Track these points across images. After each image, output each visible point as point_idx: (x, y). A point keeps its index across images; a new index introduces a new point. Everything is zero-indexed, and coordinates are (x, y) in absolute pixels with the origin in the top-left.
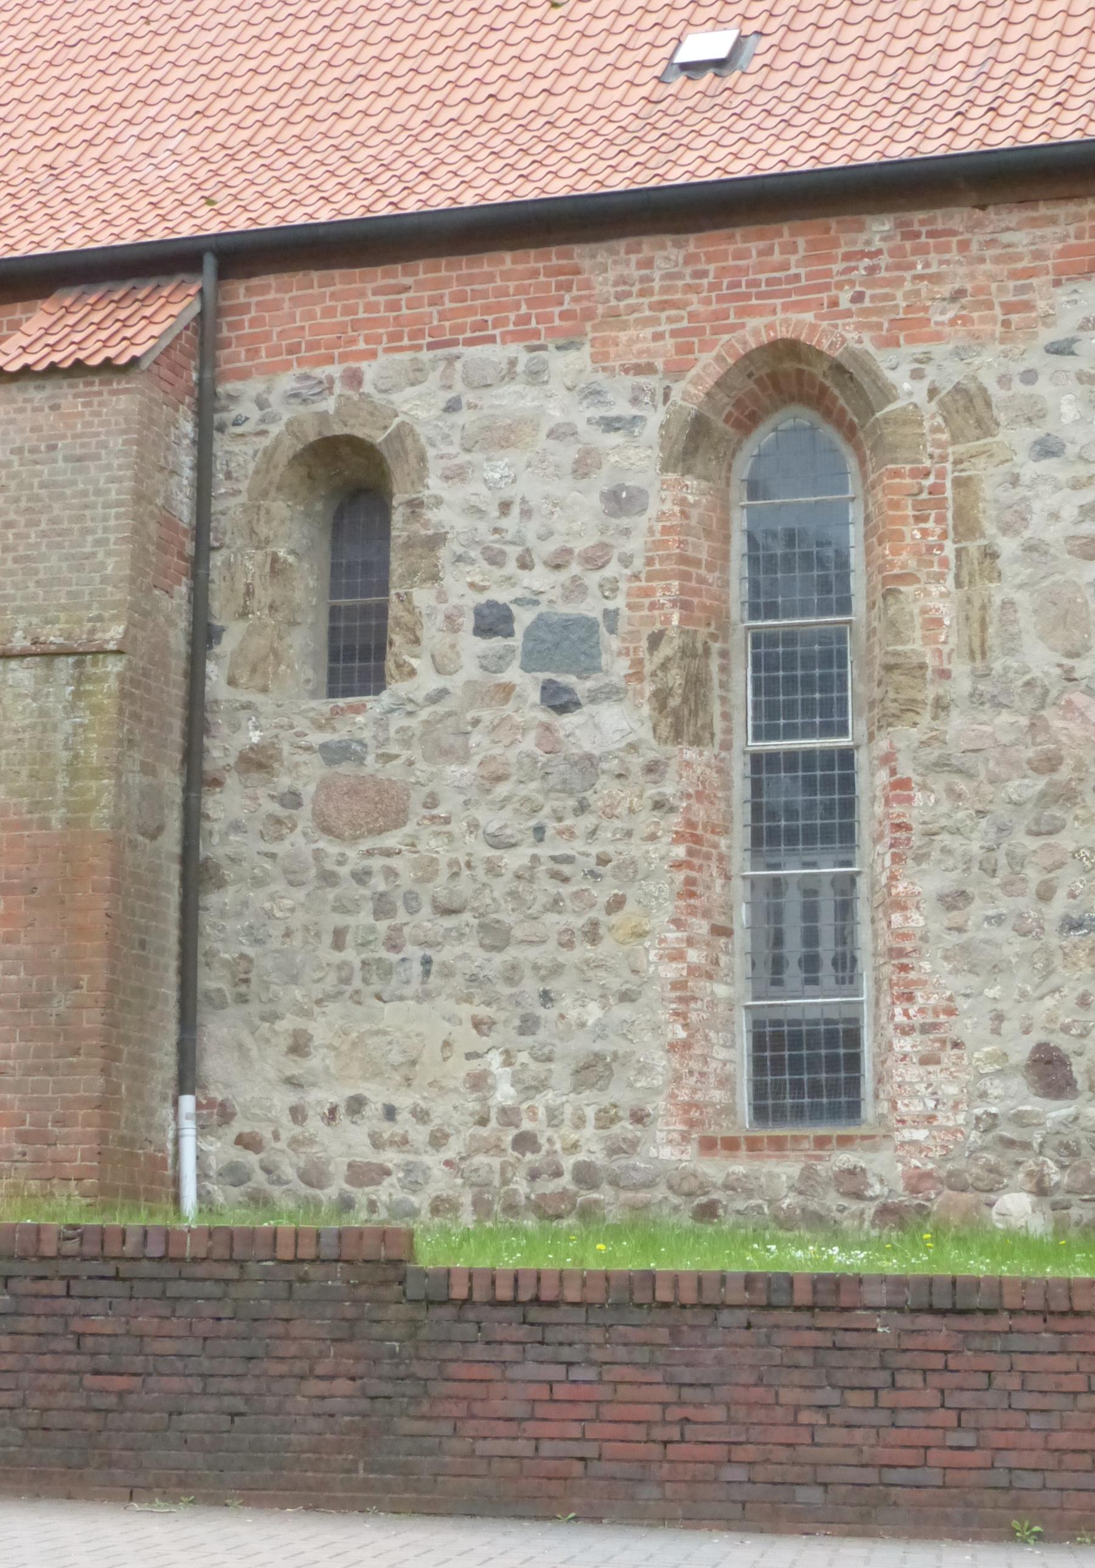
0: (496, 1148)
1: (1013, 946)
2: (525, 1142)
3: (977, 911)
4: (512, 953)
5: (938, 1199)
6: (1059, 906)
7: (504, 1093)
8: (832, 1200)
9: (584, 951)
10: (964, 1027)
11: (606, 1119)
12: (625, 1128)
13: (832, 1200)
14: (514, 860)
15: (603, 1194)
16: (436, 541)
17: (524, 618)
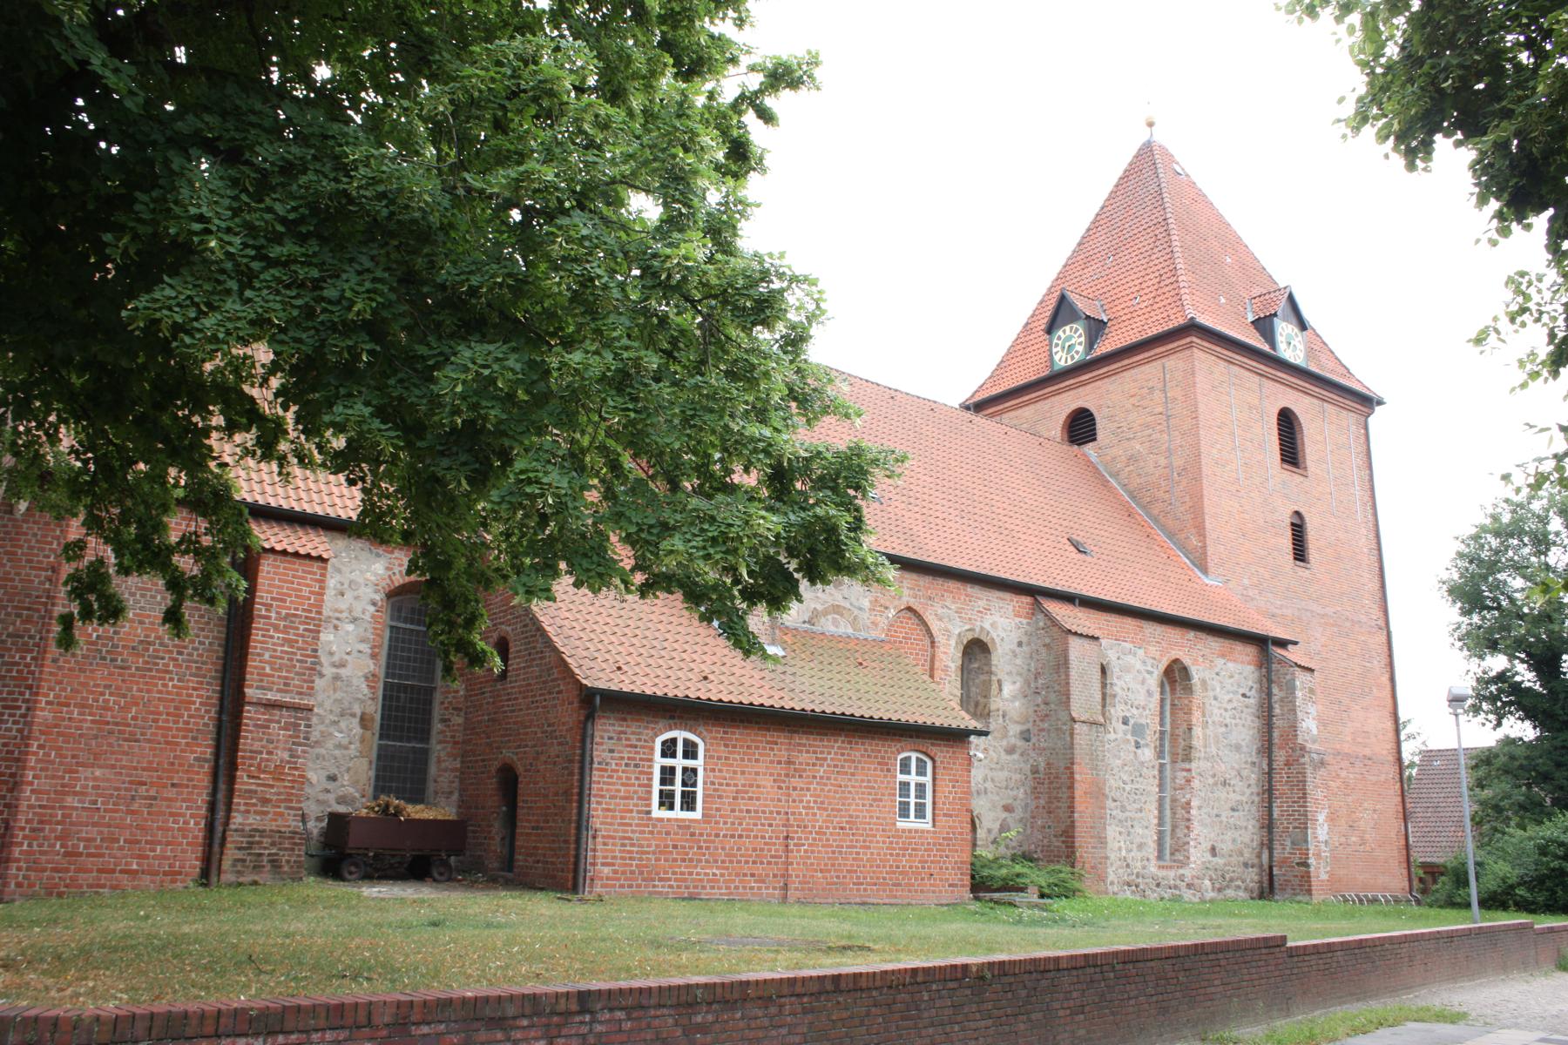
0: (1121, 867)
1: (1208, 821)
2: (1128, 866)
3: (1204, 810)
4: (1128, 814)
5: (1196, 881)
6: (1215, 811)
7: (1124, 853)
8: (1178, 882)
9: (1139, 815)
10: (1201, 839)
11: (1142, 860)
12: (1145, 862)
13: (1178, 882)
14: (1128, 788)
15: (1140, 880)
16: (1115, 696)
17: (1132, 722)
